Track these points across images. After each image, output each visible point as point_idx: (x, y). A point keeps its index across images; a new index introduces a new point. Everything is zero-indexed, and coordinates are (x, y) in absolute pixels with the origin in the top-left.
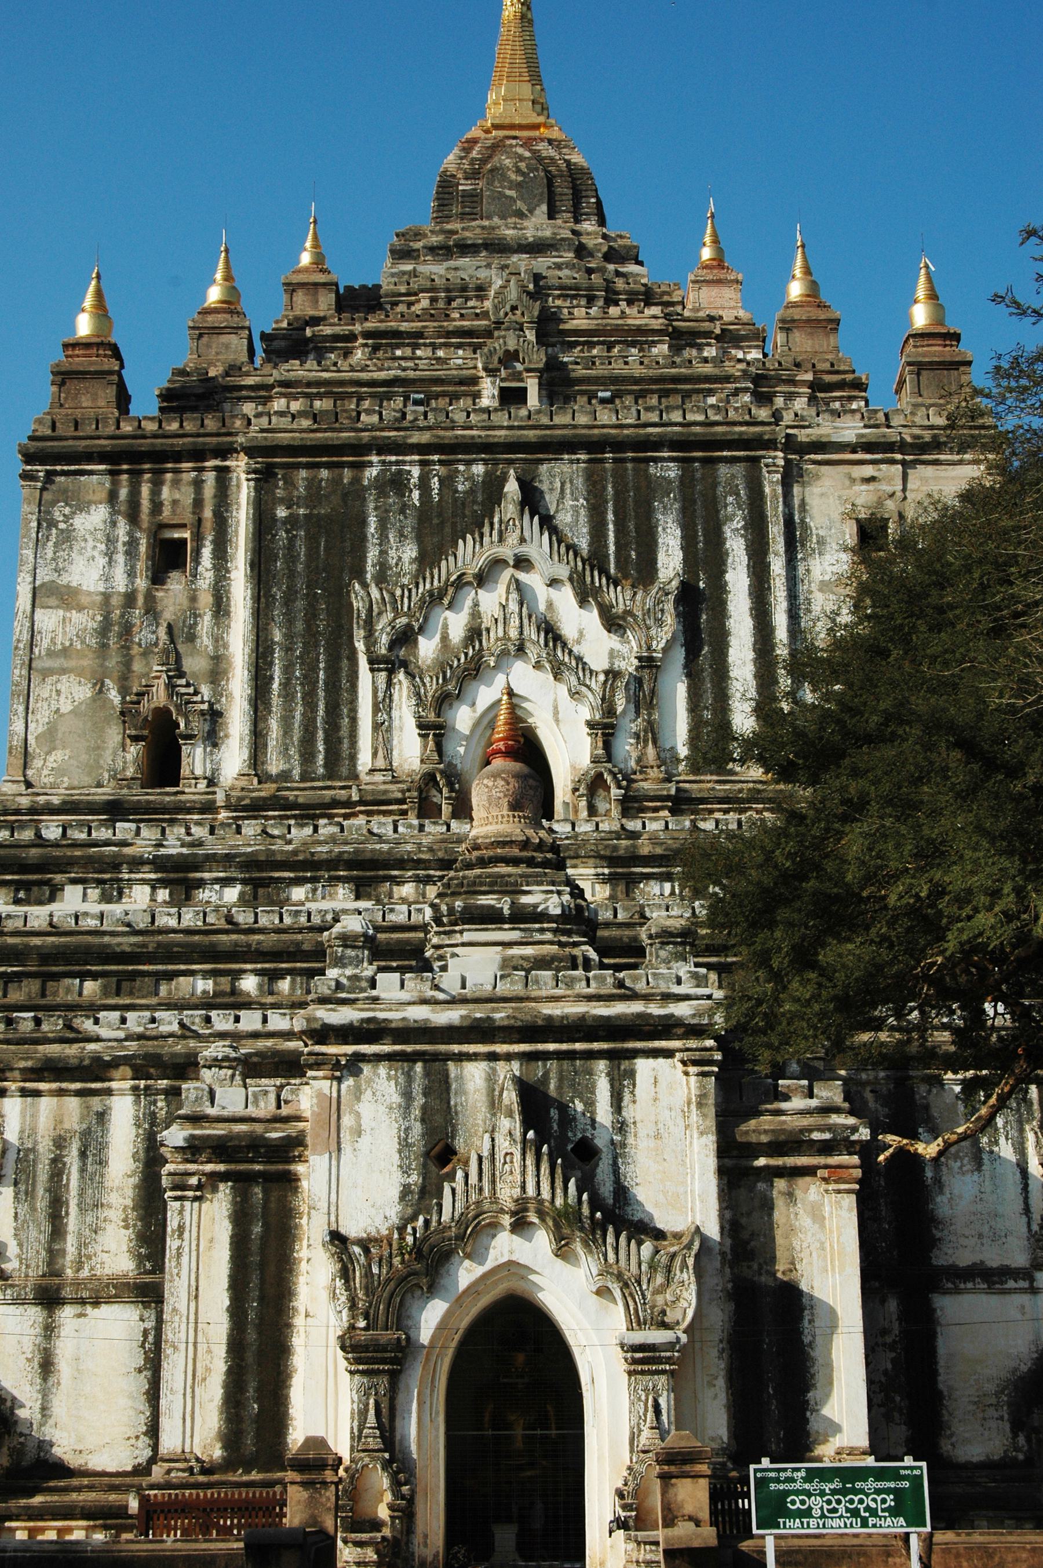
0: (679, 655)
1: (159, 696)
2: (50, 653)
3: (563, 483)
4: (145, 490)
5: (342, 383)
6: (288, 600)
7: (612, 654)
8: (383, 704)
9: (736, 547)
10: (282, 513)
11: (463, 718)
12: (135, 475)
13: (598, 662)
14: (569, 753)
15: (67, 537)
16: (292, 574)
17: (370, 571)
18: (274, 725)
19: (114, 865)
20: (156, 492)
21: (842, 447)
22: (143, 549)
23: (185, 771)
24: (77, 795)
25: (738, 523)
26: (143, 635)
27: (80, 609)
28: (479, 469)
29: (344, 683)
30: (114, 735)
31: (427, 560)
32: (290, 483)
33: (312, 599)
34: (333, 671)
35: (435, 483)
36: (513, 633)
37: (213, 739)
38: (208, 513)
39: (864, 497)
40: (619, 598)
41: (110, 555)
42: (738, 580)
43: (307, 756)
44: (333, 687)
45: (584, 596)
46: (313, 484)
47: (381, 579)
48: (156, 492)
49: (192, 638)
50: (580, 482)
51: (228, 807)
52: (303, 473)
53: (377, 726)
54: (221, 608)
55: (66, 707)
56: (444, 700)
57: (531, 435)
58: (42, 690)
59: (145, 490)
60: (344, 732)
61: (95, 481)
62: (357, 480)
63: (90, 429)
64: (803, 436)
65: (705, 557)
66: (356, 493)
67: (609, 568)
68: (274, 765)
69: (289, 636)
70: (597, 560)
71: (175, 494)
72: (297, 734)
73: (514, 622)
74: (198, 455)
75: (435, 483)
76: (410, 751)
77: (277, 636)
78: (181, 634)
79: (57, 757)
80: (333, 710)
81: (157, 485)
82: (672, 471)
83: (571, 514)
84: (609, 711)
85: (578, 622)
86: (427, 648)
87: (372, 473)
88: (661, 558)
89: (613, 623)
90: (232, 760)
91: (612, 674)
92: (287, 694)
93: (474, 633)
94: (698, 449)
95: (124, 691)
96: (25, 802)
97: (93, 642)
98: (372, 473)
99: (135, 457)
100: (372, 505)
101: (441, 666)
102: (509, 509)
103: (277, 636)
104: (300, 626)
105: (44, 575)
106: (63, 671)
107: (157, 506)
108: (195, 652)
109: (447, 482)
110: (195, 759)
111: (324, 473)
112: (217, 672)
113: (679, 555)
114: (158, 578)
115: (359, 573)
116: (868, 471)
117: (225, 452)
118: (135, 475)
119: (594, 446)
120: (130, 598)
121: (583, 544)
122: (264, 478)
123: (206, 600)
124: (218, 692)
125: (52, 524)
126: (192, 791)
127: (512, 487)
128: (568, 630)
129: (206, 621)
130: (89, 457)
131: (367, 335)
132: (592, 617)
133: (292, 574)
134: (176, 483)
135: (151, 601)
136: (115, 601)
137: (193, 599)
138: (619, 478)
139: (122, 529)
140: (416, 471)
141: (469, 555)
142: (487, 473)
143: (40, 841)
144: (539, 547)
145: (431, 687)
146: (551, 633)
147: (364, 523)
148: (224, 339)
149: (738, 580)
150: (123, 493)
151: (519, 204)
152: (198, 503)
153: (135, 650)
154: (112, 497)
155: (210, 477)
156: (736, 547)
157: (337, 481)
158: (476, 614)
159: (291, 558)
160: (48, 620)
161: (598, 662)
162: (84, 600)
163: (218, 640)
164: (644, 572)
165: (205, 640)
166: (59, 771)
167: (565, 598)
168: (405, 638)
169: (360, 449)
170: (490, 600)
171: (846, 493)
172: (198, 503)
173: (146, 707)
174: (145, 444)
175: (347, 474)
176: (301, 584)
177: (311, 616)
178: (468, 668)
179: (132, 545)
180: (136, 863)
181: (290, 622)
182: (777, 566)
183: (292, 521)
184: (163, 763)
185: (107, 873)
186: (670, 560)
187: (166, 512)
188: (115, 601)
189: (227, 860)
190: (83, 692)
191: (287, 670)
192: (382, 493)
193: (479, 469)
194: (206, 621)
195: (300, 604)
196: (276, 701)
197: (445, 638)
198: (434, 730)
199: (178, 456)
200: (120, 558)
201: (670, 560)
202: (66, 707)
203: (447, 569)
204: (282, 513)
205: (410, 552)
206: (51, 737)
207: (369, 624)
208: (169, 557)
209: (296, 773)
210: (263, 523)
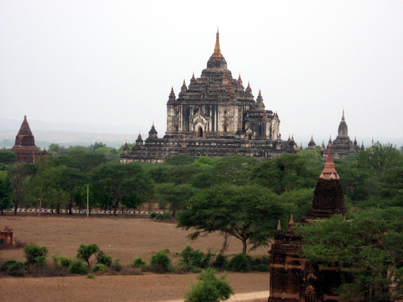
0: (211, 122)
1: (176, 125)
6: (185, 117)
9: (215, 113)
11: (196, 127)
13: (205, 123)
14: (203, 129)
15: (170, 111)
26: (175, 119)
30: (174, 127)
31: (194, 114)
37: (180, 127)
39: (225, 109)
40: (207, 118)
42: (215, 116)
45: (204, 117)
54: (181, 117)
56: (195, 125)
58: (169, 123)
65: (213, 114)
67: (207, 115)
70: (206, 115)
71: (177, 108)
74: (179, 105)
76: (192, 129)
78: (178, 119)
83: (204, 110)
85: (204, 119)
86: (194, 121)
90: (181, 129)
91: (206, 124)
93: (197, 120)
99: (174, 105)
101: (195, 123)
109: (196, 108)
110: (179, 129)
112: (180, 122)
114: (176, 115)
117: (181, 105)
119: (206, 105)
120: (174, 116)
121: (205, 113)
122: (183, 107)
126: (179, 132)
128: (203, 120)
130: (171, 105)
146: (202, 120)
149: (215, 116)
154: (173, 108)
156: (215, 113)
160: (169, 118)
161: (205, 123)
163: (180, 120)
165: (180, 120)
169: (190, 105)
170: (198, 117)
178: (196, 123)
184: (177, 130)
206: (169, 127)
208: (178, 113)
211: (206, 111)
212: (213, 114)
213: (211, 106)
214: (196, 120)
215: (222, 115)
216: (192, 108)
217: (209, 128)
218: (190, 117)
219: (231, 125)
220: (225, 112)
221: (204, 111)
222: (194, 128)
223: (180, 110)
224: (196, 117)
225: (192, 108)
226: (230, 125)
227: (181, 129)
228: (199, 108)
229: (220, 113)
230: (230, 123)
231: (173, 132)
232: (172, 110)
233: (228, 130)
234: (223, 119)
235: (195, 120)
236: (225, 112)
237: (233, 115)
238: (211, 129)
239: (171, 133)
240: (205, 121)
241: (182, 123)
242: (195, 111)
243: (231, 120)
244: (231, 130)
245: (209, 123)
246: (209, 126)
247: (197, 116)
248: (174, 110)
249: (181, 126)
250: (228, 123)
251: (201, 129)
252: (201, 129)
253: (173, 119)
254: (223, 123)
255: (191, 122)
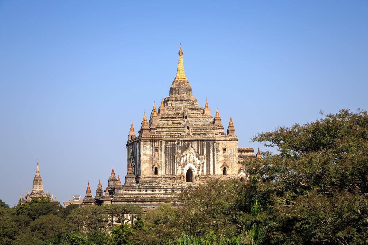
0: (206, 162)
1: (156, 166)
2: (145, 161)
3: (195, 143)
4: (153, 143)
5: (170, 128)
6: (168, 156)
7: (199, 163)
8: (177, 168)
9: (211, 151)
10: (167, 147)
12: (152, 142)
13: (198, 163)
14: (195, 173)
15: (146, 149)
16: (168, 153)
17: (176, 153)
18: (167, 169)
19: (160, 188)
20: (154, 144)
21: (222, 141)
22: (153, 150)
23: (158, 174)
24: (149, 176)
25: (212, 149)
26: (154, 159)
27: (148, 156)
28: (187, 142)
29: (174, 165)
30: (151, 169)
31: (182, 152)
32: (168, 143)
33: (170, 156)
34: (173, 163)
35: (182, 144)
36: (190, 161)
38: (160, 146)
39: (224, 146)
40: (200, 157)
41: (150, 150)
43: (170, 172)
44: (173, 165)
45: (197, 156)
46: (170, 143)
47: (177, 154)
48: (154, 144)
49: (159, 160)
50: (196, 144)
51: (164, 178)
52: (169, 142)
53: (177, 170)
54: (161, 156)
55: (147, 167)
56: (184, 167)
57: (192, 139)
59: (153, 143)
60: (174, 170)
61: (148, 142)
62: (175, 143)
63: (147, 136)
64: (218, 139)
65: (208, 152)
66: (174, 145)
67: (200, 153)
68: (167, 173)
69: (168, 160)
70: (198, 152)
71: (157, 144)
72: (169, 170)
73: (190, 159)
74: (159, 140)
75: (182, 144)
76: (180, 172)
77: (167, 160)
79: (146, 172)
80: (173, 168)
81: (155, 143)
82: (205, 143)
83: (196, 147)
84: (199, 169)
85: (196, 159)
86: (182, 162)
87: (176, 143)
88: (204, 152)
89: (199, 159)
92: (168, 166)
93: (186, 160)
94: (208, 141)
95: (152, 165)
96: (144, 177)
97: (149, 160)
98: (176, 143)
99: (152, 140)
100: (176, 146)
101: (183, 164)
102: (190, 147)
103: (167, 160)
104: (169, 159)
105: (144, 153)
106: (146, 163)
107: (155, 146)
108: (159, 161)
109: (184, 144)
110: (159, 172)
111: (171, 142)
112: (161, 163)
113: (206, 152)
115: (175, 153)
116: (224, 143)
118: (152, 142)
119: (198, 140)
120: (152, 155)
122: (166, 143)
123: (160, 156)
124: (161, 166)
125: (144, 147)
126: (160, 176)
127: (190, 145)
128: (195, 160)
129: (160, 158)
130: (148, 140)
131: (170, 117)
132: (197, 158)
133: (168, 153)
134: (156, 143)
135: (154, 155)
136: (151, 155)
137: (159, 155)
138: (200, 143)
139: (151, 147)
140: (180, 142)
141: (186, 152)
142: (188, 143)
143: (153, 186)
144: (192, 151)
145: (182, 166)
147: (175, 148)
148: (156, 120)
149: (211, 155)
150: (151, 144)
151: (183, 92)
152: (159, 145)
153: (153, 161)
155: (160, 142)
156: (211, 151)
157: (173, 143)
158: (186, 158)
159: (168, 152)
160: (144, 157)
162: (148, 155)
164: (203, 154)
165: (160, 160)
166: (146, 173)
167: (195, 157)
168: (180, 160)
171: (222, 145)
172: (159, 145)
173: (155, 167)
174: (154, 139)
175: (174, 143)
176: (169, 154)
177: (170, 158)
178: (186, 163)
179: (152, 149)
180: (162, 189)
181: (168, 158)
182: (215, 153)
183: (168, 147)
184: (156, 173)
185: (160, 189)
186: (205, 153)
187: (156, 146)
188: (151, 155)
189: (170, 188)
190: (148, 165)
191: (168, 163)
192: (177, 145)
193: (187, 142)
194: (160, 158)
195: (169, 156)
196: (167, 166)
197: (183, 160)
198: (182, 170)
199: (157, 140)
200: (151, 151)
201: (205, 153)
202: (147, 167)
203: (184, 153)
204: (167, 147)
205: (180, 151)
206: (145, 170)
207: (176, 159)
208: (156, 150)
209: (169, 174)
210: (166, 148)
211: (198, 147)
212: (208, 152)
213: (205, 143)
214: (185, 160)
215: (221, 152)
216: (178, 144)
217: (203, 171)
218: (176, 156)
219: (233, 167)
220: (225, 150)
221: (195, 148)
222: (182, 170)
223: (161, 147)
224: (185, 156)
225: (178, 144)
226: (231, 166)
227: (161, 172)
228: (188, 144)
229: (218, 150)
230: (232, 164)
231: (151, 176)
232: (148, 147)
233: (228, 172)
234: (221, 159)
235: (183, 160)
236: (225, 150)
237: (235, 153)
238: (206, 172)
239: (148, 177)
240: (198, 162)
241: (163, 164)
242: (185, 148)
243: (232, 160)
244: (232, 173)
245: (203, 164)
246: (203, 168)
247: (187, 155)
248: (152, 146)
249: (161, 169)
250: (229, 164)
251: (190, 172)
252: (190, 172)
253: (150, 159)
254: (221, 164)
255: (177, 163)
